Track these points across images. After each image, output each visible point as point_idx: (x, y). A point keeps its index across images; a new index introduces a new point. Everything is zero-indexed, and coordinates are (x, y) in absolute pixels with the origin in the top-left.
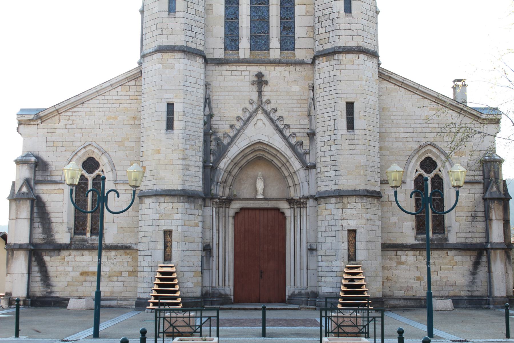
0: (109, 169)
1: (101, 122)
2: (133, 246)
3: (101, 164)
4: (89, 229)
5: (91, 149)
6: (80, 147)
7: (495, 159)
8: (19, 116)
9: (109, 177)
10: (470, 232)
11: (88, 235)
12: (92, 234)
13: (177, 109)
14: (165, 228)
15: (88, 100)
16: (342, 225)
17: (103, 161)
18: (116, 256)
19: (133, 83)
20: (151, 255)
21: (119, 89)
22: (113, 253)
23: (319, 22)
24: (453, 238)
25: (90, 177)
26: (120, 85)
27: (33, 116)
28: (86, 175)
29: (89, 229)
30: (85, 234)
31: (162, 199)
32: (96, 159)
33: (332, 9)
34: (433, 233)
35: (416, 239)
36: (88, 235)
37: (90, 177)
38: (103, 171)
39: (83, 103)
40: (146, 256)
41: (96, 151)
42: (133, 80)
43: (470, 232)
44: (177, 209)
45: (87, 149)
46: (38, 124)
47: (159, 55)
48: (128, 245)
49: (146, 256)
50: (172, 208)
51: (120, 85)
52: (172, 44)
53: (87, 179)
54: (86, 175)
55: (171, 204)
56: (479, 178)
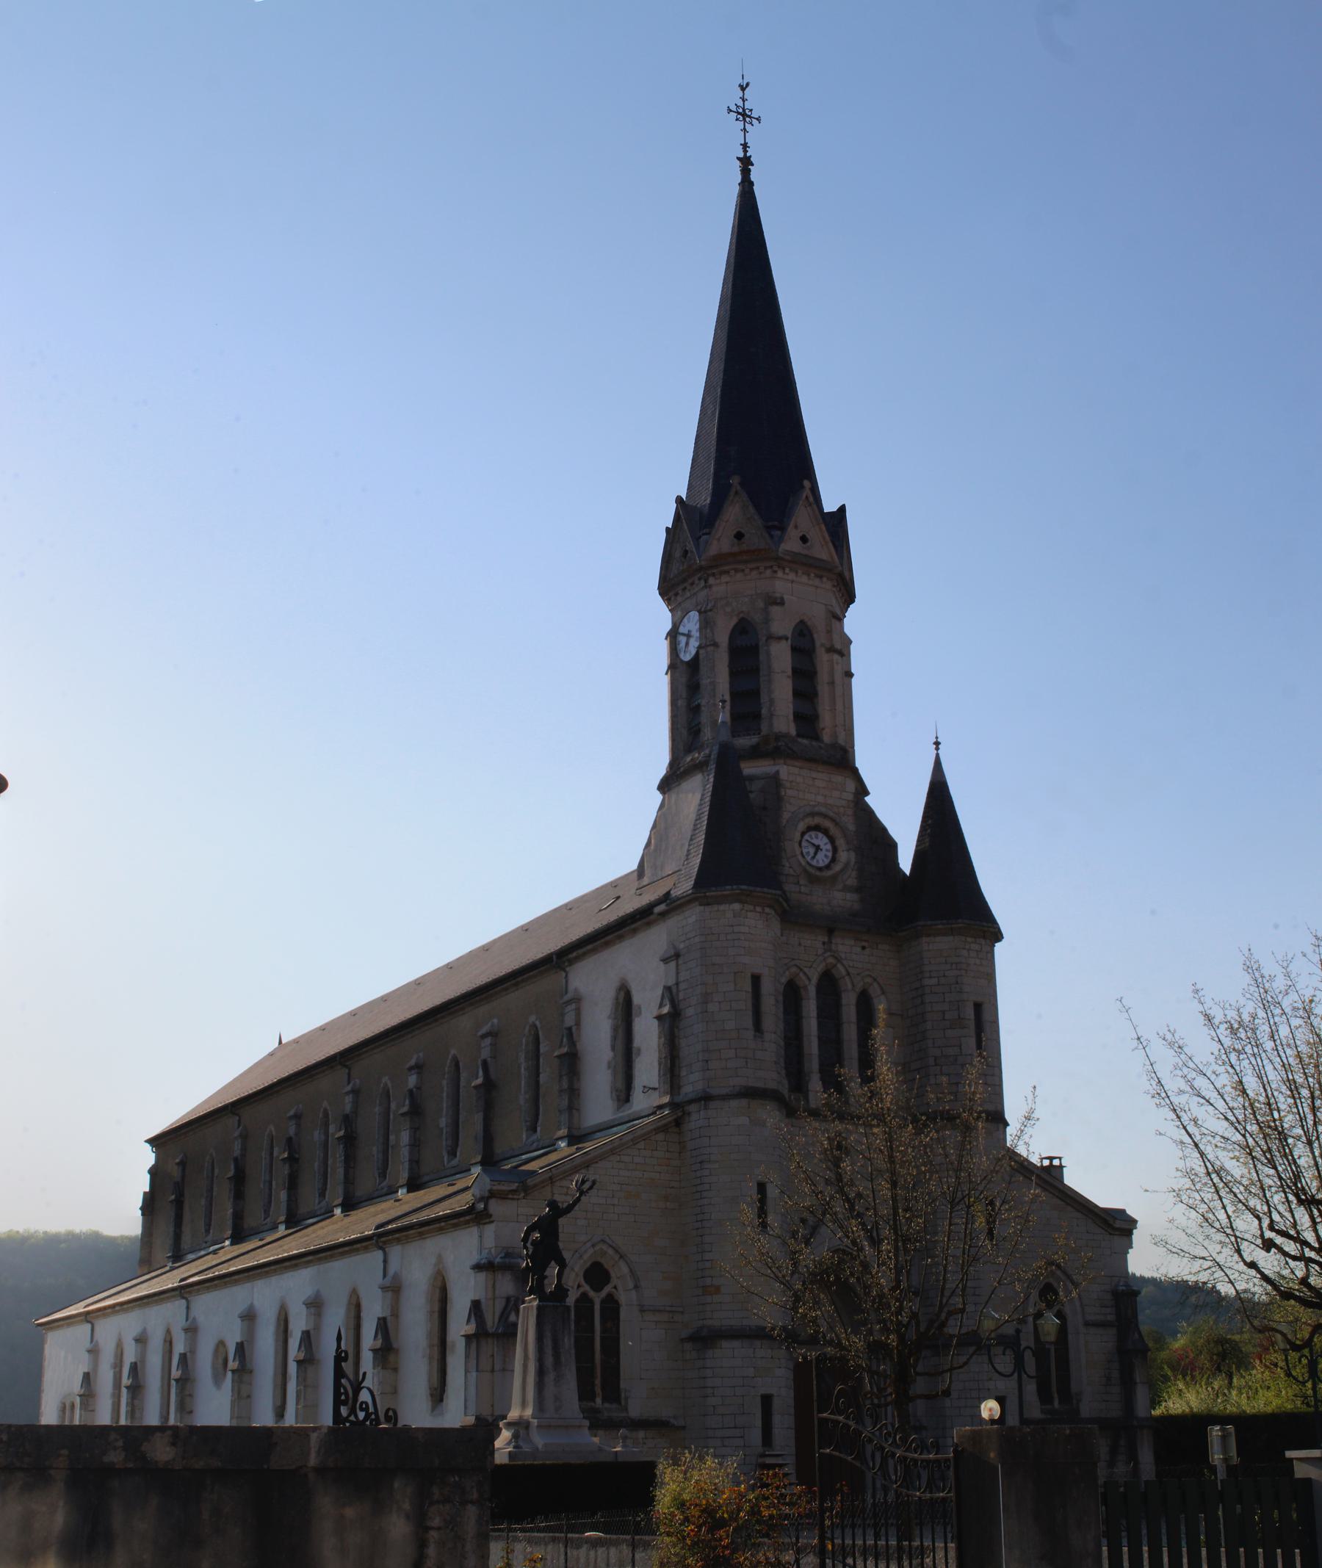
0: (631, 1285)
1: (616, 1202)
2: (672, 1421)
3: (613, 1274)
4: (598, 1390)
5: (603, 1247)
6: (585, 1243)
7: (1134, 1290)
8: (495, 1183)
9: (626, 1298)
10: (1104, 1401)
11: (599, 1401)
12: (605, 1399)
13: (772, 1192)
14: (763, 1391)
15: (597, 1162)
16: (989, 1389)
17: (619, 1273)
18: (646, 1438)
19: (661, 1136)
20: (742, 1437)
21: (641, 1145)
22: (641, 1434)
23: (936, 1065)
24: (1086, 1410)
25: (597, 1298)
26: (644, 1140)
27: (516, 1184)
28: (592, 1294)
29: (598, 1390)
30: (593, 1400)
31: (758, 1343)
32: (606, 1266)
33: (961, 1049)
34: (1060, 1403)
35: (1043, 1411)
36: (599, 1401)
37: (597, 1298)
38: (615, 1287)
39: (588, 1166)
40: (728, 1438)
41: (611, 1251)
42: (663, 1131)
43: (1104, 1401)
44: (779, 1359)
45: (597, 1248)
46: (518, 1199)
47: (744, 1102)
48: (664, 1419)
49: (728, 1438)
50: (772, 1358)
51: (644, 1140)
52: (760, 1084)
53: (591, 1301)
54: (592, 1294)
55: (770, 1351)
56: (1111, 1318)
